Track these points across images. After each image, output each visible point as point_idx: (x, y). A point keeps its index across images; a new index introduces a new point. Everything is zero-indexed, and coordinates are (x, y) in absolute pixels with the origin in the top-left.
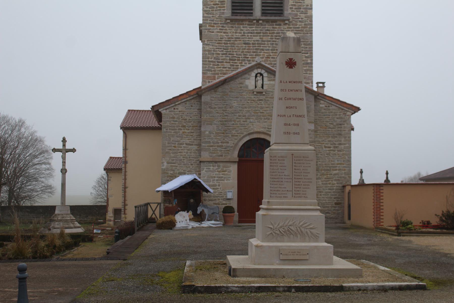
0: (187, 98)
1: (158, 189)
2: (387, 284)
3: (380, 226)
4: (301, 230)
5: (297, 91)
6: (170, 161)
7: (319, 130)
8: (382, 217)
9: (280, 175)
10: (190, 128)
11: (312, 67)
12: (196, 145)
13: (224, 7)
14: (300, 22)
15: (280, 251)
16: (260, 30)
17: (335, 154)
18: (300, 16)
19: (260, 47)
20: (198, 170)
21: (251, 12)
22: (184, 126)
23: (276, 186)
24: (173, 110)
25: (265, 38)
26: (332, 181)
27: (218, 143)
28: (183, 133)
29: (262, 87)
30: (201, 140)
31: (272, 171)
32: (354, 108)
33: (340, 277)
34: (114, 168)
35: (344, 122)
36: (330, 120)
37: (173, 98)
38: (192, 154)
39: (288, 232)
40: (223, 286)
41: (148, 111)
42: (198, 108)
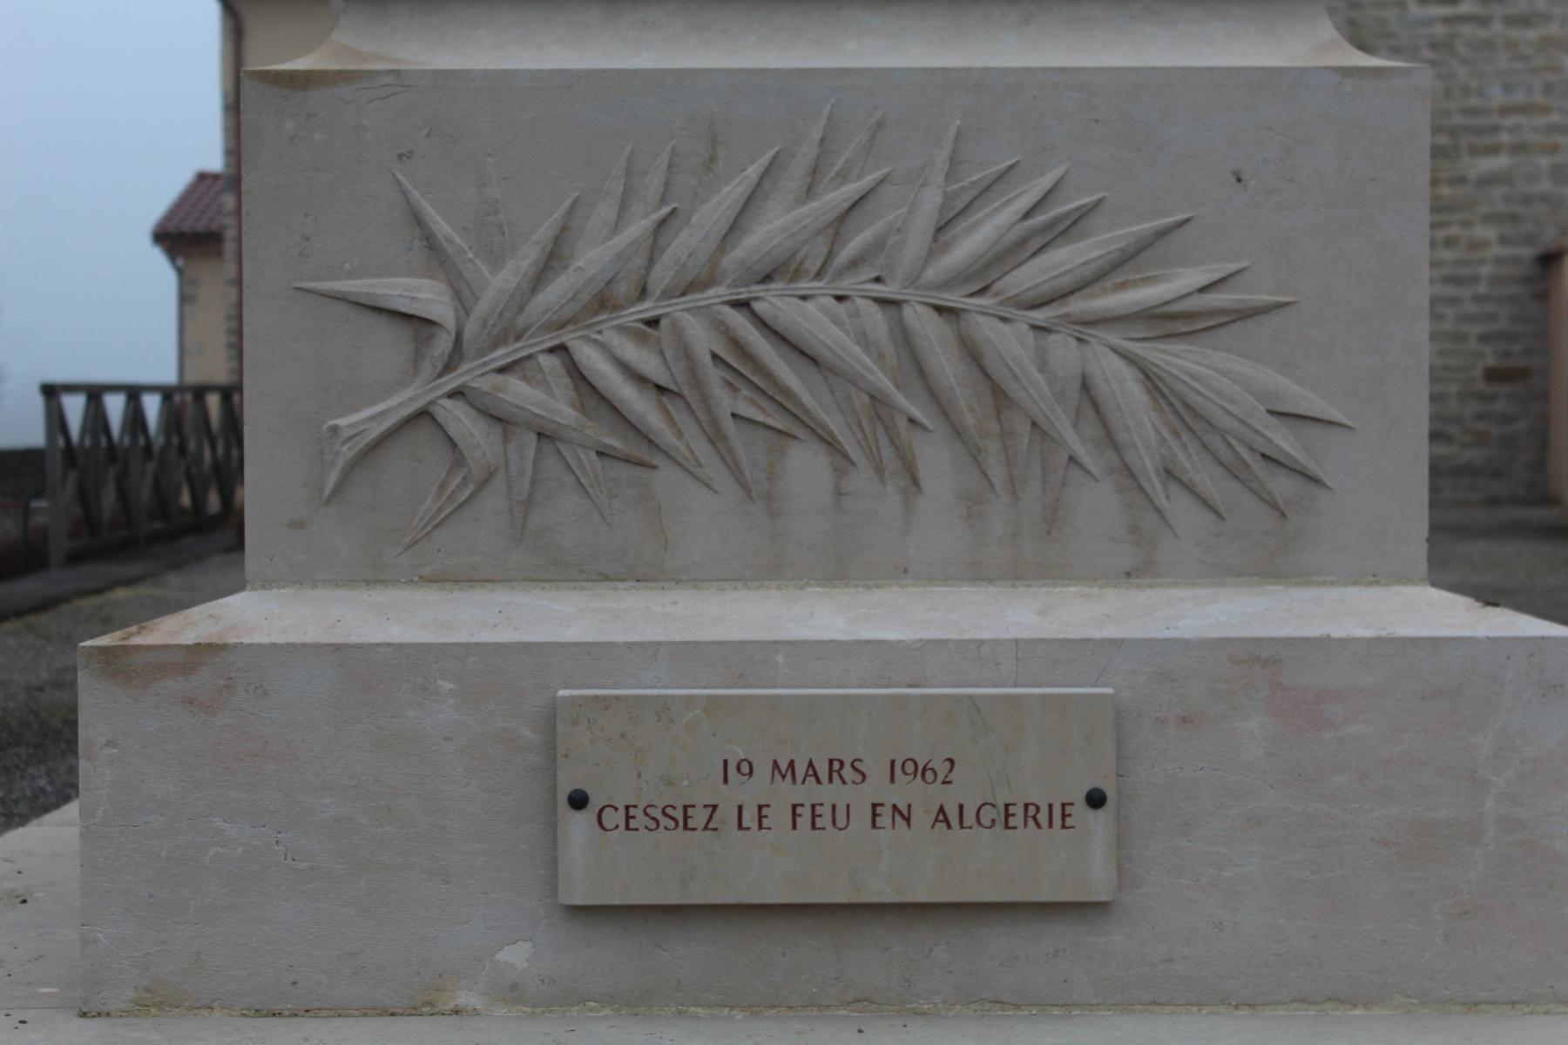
4: (972, 354)
17: (1489, 45)
26: (1467, 224)
39: (726, 402)
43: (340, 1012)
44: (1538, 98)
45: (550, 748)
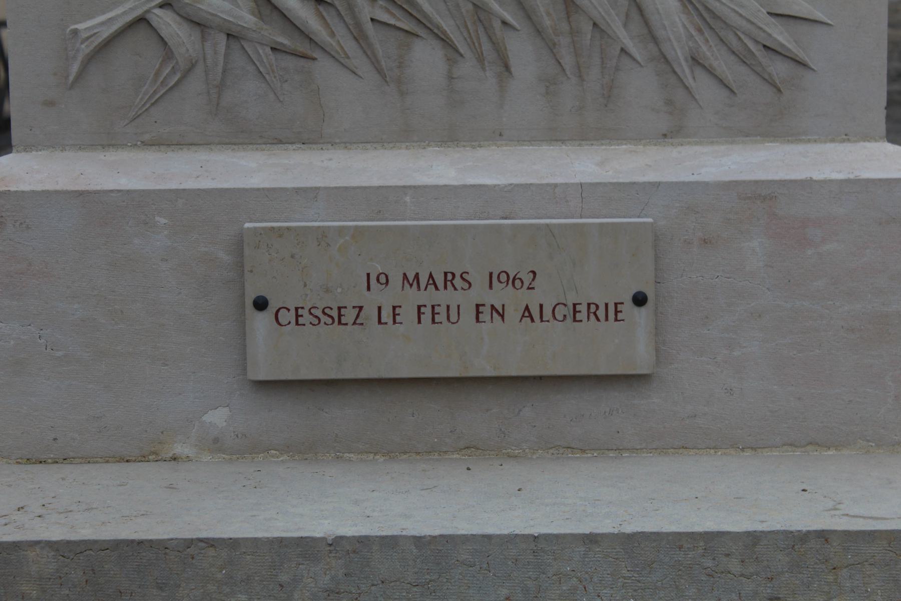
15: (248, 274)
43: (88, 460)
45: (240, 265)
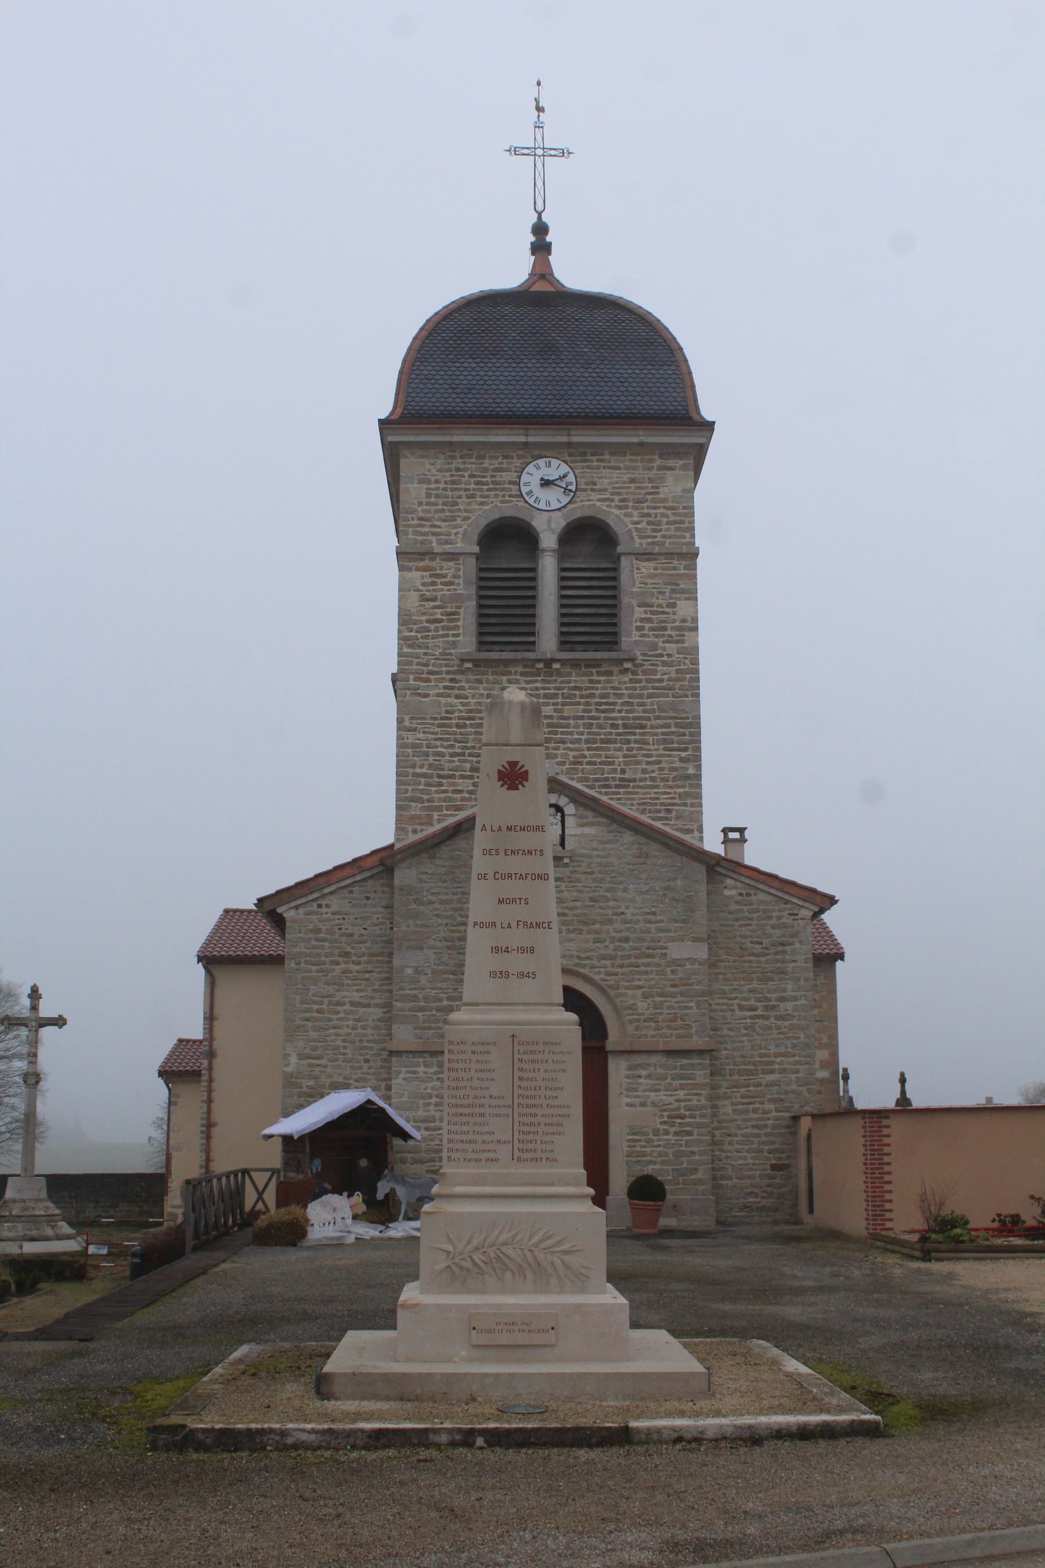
0: (353, 876)
1: (268, 1131)
2: (763, 1419)
3: (884, 1233)
5: (530, 852)
6: (307, 1051)
7: (723, 961)
8: (888, 1206)
9: (476, 1097)
10: (363, 959)
11: (700, 786)
12: (378, 1006)
13: (457, 627)
14: (664, 664)
16: (555, 688)
17: (770, 1028)
18: (664, 649)
19: (556, 733)
20: (385, 1076)
21: (532, 639)
22: (347, 954)
23: (465, 1128)
24: (315, 908)
25: (568, 711)
26: (762, 1103)
27: (440, 1000)
28: (344, 972)
29: (562, 844)
30: (391, 991)
31: (455, 1084)
32: (818, 898)
33: (642, 1399)
34: (185, 1070)
35: (792, 936)
36: (752, 931)
37: (317, 876)
38: (369, 1031)
40: (271, 1430)
41: (250, 911)
42: (384, 903)
44: (790, 1050)
